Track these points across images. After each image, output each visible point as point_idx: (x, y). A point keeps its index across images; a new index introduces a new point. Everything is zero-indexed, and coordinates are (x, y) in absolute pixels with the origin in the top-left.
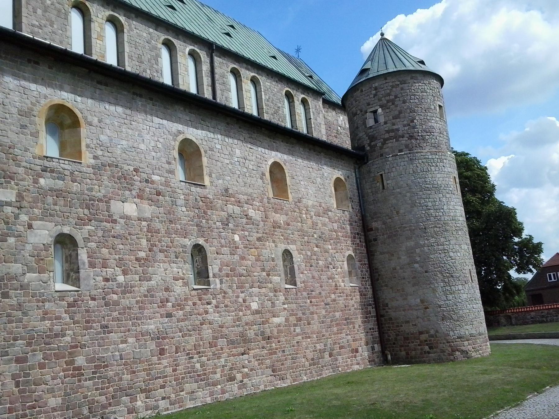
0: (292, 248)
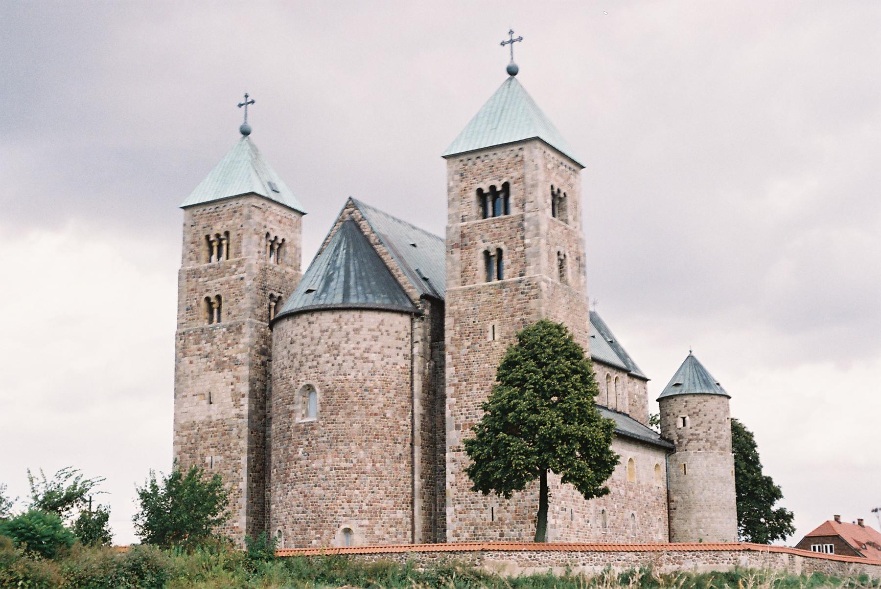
0: (635, 512)
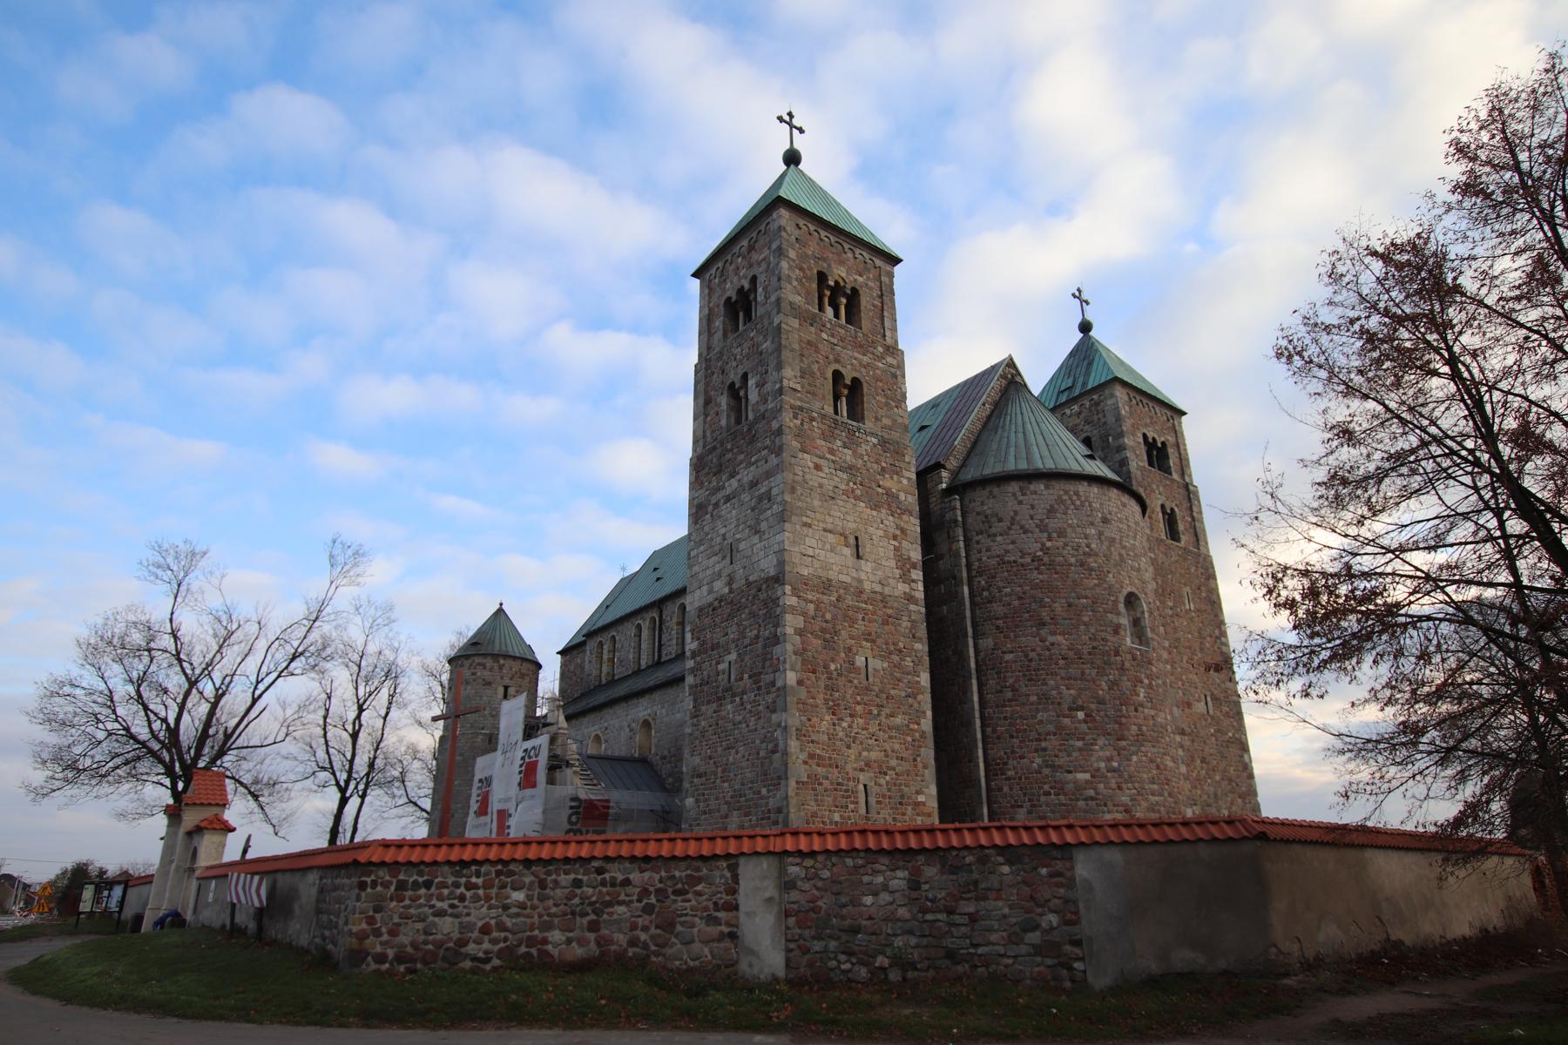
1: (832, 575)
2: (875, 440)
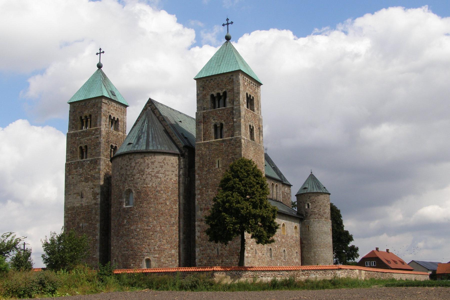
0: (285, 249)
1: (74, 205)
2: (89, 162)
